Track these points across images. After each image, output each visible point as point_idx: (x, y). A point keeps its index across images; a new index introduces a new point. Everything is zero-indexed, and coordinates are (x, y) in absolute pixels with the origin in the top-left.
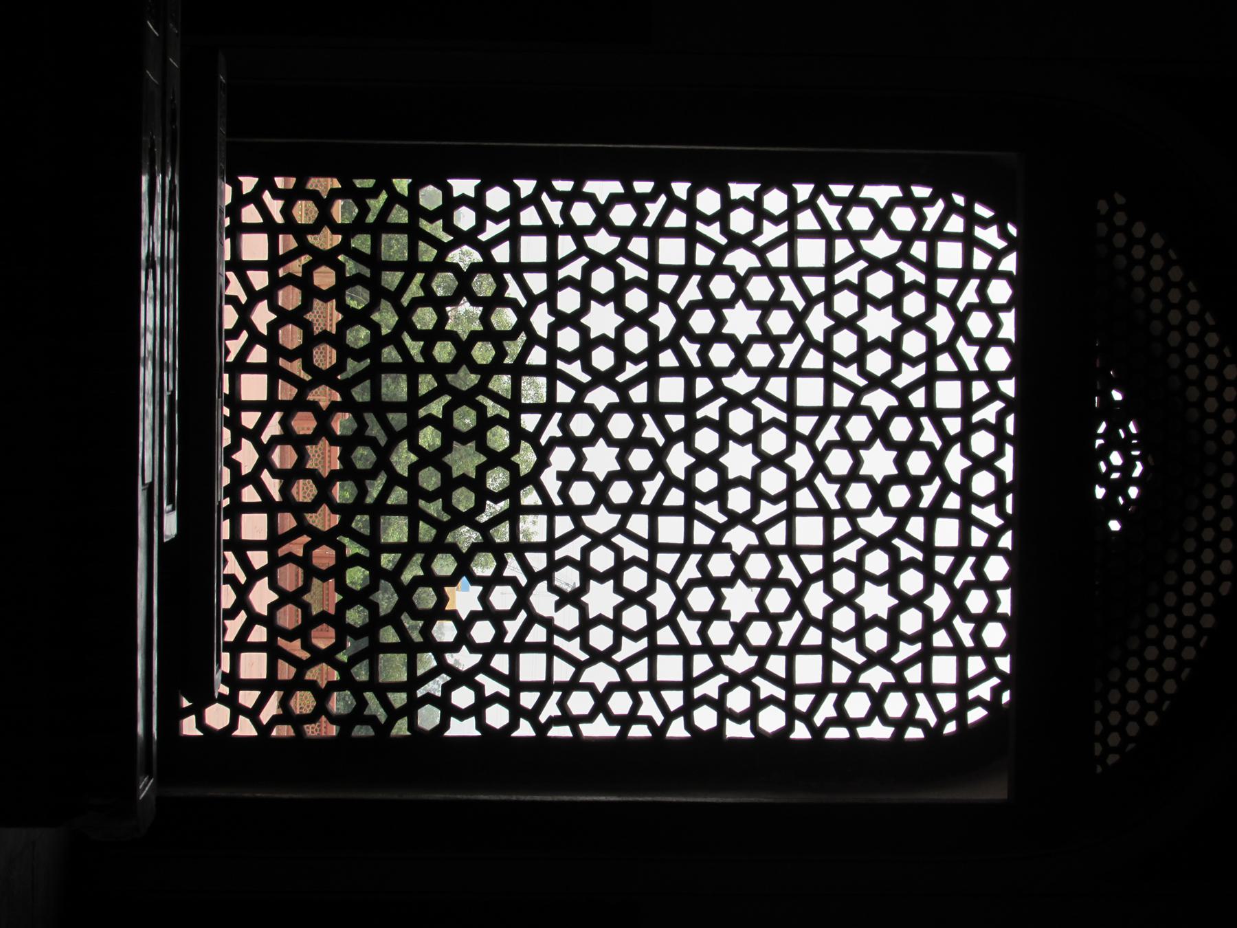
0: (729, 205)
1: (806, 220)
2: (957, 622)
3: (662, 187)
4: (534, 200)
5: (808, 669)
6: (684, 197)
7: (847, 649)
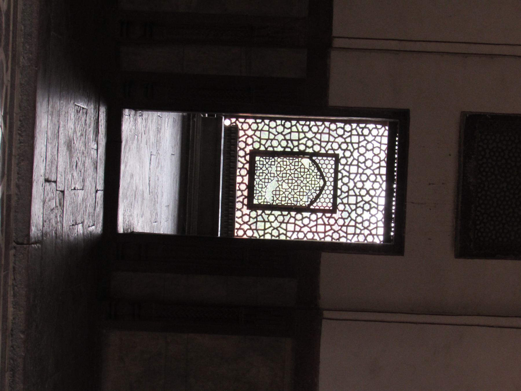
0: (337, 128)
1: (354, 132)
6: (328, 126)
7: (360, 226)
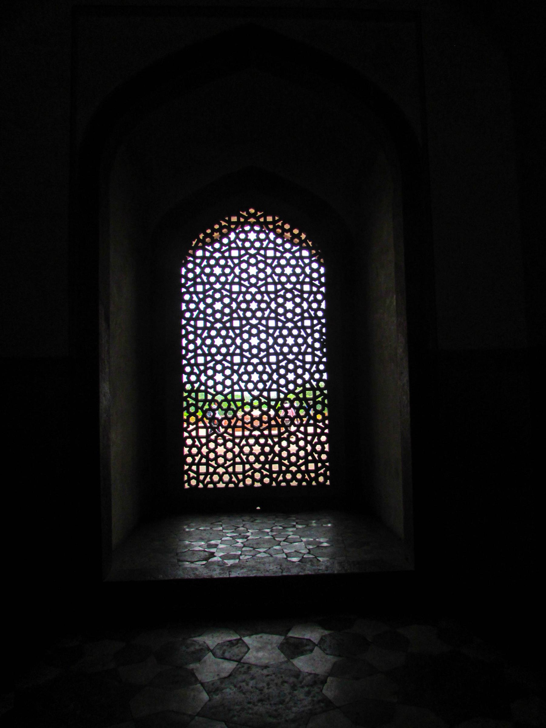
2: (295, 320)
3: (185, 399)
4: (190, 432)
5: (308, 358)
